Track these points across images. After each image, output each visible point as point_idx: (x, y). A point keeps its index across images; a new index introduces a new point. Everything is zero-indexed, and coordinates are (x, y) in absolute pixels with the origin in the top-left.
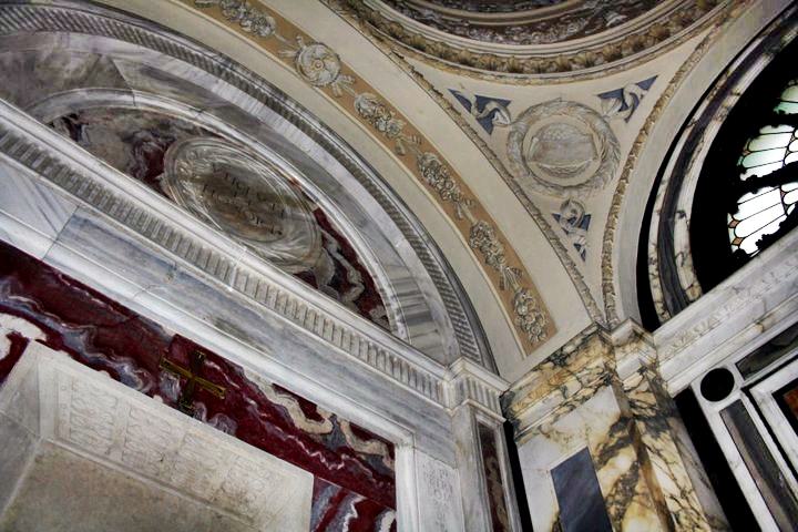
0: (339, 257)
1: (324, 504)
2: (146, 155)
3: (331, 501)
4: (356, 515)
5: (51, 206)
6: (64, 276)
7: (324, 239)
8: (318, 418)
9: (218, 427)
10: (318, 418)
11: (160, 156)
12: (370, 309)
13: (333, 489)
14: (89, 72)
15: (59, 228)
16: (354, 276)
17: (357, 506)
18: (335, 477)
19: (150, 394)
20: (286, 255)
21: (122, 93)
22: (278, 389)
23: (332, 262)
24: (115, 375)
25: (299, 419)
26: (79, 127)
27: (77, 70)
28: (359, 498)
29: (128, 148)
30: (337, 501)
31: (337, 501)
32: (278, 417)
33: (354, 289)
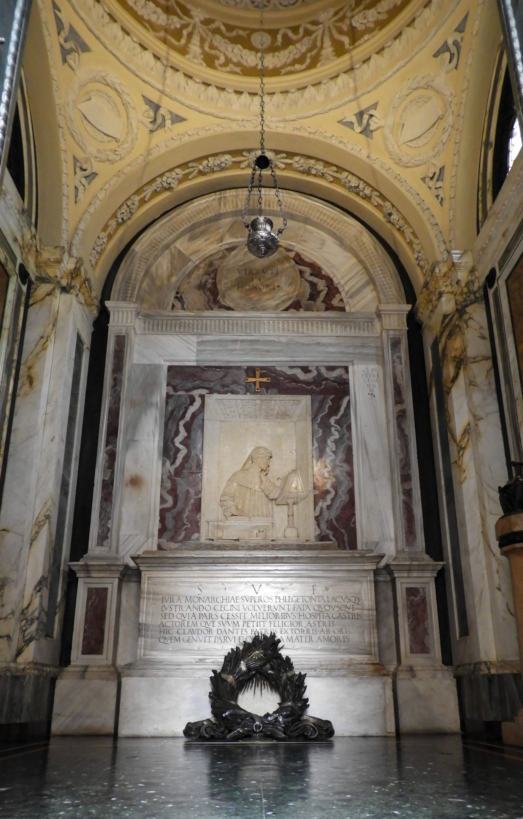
0: (312, 278)
1: (317, 405)
2: (210, 289)
3: (319, 402)
4: (331, 403)
5: (188, 343)
6: (205, 367)
7: (301, 272)
9: (271, 394)
11: (215, 284)
12: (331, 300)
13: (321, 397)
15: (195, 350)
16: (321, 285)
17: (331, 400)
18: (320, 393)
19: (245, 394)
20: (283, 298)
21: (188, 263)
22: (291, 367)
23: (308, 284)
24: (233, 392)
25: (302, 376)
26: (181, 297)
27: (168, 267)
28: (332, 397)
29: (201, 292)
30: (322, 403)
31: (322, 403)
32: (294, 379)
33: (321, 294)
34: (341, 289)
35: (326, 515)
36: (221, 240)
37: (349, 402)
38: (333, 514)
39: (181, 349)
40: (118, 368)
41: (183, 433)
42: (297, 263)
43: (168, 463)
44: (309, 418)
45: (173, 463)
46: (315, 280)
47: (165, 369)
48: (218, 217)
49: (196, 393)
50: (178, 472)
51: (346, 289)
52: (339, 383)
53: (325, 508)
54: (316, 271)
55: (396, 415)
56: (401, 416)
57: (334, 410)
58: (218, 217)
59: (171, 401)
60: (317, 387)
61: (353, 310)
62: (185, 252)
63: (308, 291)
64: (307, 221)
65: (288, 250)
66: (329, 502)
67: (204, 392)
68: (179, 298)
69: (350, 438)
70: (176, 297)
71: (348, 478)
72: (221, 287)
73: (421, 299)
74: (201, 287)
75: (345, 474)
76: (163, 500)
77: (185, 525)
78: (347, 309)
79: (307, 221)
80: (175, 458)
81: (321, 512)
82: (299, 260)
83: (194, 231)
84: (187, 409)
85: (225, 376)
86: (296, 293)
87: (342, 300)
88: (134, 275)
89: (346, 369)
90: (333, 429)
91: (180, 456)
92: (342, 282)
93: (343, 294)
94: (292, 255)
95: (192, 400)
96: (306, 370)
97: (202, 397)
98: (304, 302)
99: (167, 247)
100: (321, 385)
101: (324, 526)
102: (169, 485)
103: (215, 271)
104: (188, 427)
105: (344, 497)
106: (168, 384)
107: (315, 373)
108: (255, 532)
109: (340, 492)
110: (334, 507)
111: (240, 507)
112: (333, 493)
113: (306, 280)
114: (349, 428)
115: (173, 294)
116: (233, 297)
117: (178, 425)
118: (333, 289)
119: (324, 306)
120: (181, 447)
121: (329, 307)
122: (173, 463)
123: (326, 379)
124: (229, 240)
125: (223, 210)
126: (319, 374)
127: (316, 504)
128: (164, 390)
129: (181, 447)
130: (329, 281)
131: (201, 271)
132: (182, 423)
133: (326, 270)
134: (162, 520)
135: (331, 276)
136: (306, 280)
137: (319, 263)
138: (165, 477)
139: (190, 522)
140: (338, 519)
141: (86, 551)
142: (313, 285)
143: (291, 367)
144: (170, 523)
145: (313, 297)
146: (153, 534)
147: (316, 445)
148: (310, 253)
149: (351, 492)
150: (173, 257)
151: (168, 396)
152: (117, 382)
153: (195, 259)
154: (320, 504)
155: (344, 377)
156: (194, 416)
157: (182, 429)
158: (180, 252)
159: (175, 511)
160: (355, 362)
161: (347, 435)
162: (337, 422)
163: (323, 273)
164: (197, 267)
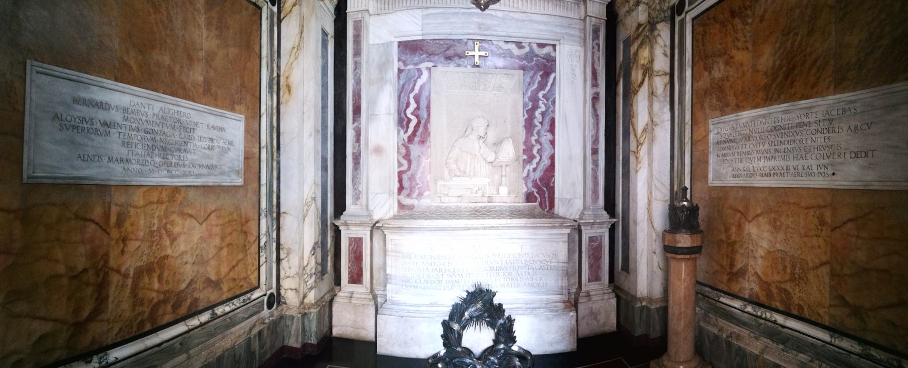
1: (528, 79)
8: (522, 47)
10: (522, 47)
13: (531, 73)
18: (532, 68)
37: (555, 78)
38: (538, 175)
44: (521, 92)
47: (396, 45)
52: (548, 60)
53: (531, 170)
56: (595, 98)
57: (542, 86)
66: (534, 166)
69: (553, 111)
81: (528, 174)
85: (448, 49)
89: (554, 46)
90: (541, 102)
101: (530, 185)
105: (546, 162)
106: (399, 60)
107: (527, 49)
108: (476, 189)
109: (544, 158)
110: (539, 170)
112: (538, 158)
114: (554, 102)
123: (537, 56)
127: (524, 167)
128: (396, 65)
147: (526, 116)
149: (552, 158)
154: (528, 167)
155: (553, 54)
160: (562, 42)
162: (544, 96)
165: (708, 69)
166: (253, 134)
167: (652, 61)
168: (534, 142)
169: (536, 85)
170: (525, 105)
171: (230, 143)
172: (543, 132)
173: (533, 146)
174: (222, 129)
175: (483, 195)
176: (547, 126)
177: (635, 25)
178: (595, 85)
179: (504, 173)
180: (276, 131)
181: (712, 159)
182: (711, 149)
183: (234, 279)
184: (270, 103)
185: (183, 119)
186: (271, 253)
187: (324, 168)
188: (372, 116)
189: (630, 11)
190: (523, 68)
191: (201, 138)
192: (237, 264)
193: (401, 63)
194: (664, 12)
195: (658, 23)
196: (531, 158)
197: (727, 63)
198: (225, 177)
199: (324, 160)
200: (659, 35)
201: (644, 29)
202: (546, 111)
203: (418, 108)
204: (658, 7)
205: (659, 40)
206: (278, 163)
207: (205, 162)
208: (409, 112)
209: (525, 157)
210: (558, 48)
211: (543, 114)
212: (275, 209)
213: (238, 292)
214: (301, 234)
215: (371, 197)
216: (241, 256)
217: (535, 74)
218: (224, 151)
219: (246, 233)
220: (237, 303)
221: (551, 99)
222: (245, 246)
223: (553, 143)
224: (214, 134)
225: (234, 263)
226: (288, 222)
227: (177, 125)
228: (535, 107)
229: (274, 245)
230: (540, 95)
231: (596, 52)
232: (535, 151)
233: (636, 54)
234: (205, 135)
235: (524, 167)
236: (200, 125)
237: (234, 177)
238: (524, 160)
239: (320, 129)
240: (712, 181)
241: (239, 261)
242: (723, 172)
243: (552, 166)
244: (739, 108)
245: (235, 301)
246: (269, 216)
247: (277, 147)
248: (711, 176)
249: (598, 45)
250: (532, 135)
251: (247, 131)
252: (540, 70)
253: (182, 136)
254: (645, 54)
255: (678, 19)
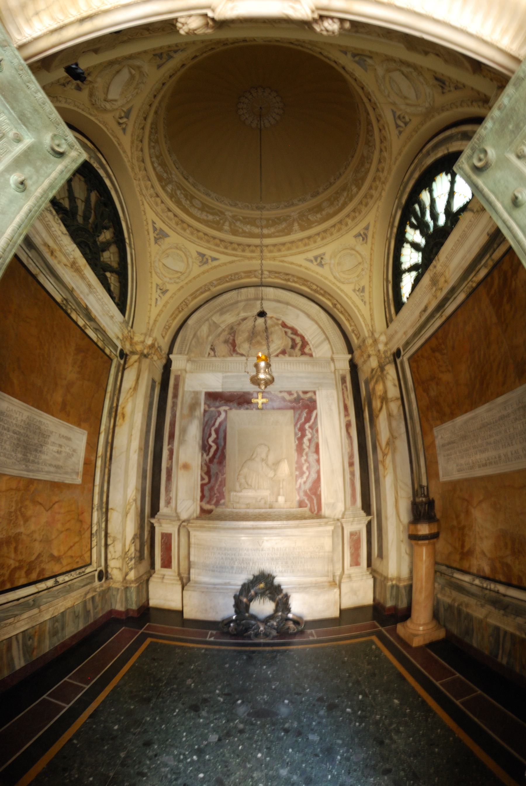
1: (297, 416)
7: (286, 333)
11: (234, 340)
14: (209, 329)
16: (298, 340)
18: (299, 408)
22: (281, 392)
31: (300, 415)
34: (309, 343)
35: (303, 487)
36: (238, 314)
39: (213, 380)
40: (175, 396)
41: (214, 436)
42: (283, 327)
43: (205, 455)
45: (208, 455)
46: (294, 337)
48: (237, 302)
49: (222, 409)
50: (211, 460)
51: (313, 343)
52: (311, 402)
54: (295, 332)
55: (345, 424)
56: (348, 425)
57: (307, 420)
58: (237, 302)
59: (207, 414)
60: (297, 404)
61: (317, 356)
62: (217, 322)
63: (290, 343)
64: (287, 304)
65: (278, 319)
66: (305, 479)
67: (227, 408)
68: (213, 349)
69: (317, 438)
70: (211, 349)
71: (317, 464)
72: (238, 342)
73: (357, 353)
74: (226, 342)
75: (315, 461)
76: (202, 479)
77: (215, 494)
78: (314, 354)
79: (287, 304)
80: (209, 451)
81: (300, 487)
82: (284, 325)
83: (222, 311)
84: (216, 419)
86: (283, 345)
87: (310, 349)
88: (187, 338)
89: (315, 393)
91: (212, 450)
92: (310, 339)
93: (311, 346)
94: (280, 322)
95: (219, 414)
96: (290, 393)
97: (226, 411)
98: (288, 350)
99: (207, 320)
100: (299, 403)
102: (205, 469)
103: (234, 333)
104: (217, 431)
105: (314, 476)
106: (205, 404)
107: (295, 395)
111: (249, 483)
112: (307, 473)
113: (289, 337)
114: (317, 431)
115: (209, 347)
116: (244, 348)
117: (210, 430)
118: (305, 343)
119: (299, 353)
120: (212, 444)
121: (303, 353)
122: (208, 455)
123: (302, 399)
124: (243, 315)
125: (239, 299)
126: (298, 396)
129: (212, 444)
130: (302, 338)
131: (226, 333)
132: (213, 429)
133: (300, 331)
134: (202, 491)
135: (303, 334)
136: (289, 337)
137: (296, 327)
138: (203, 463)
139: (219, 493)
140: (311, 489)
141: (158, 511)
142: (293, 340)
143: (281, 392)
144: (207, 493)
145: (293, 347)
146: (197, 499)
147: (297, 442)
148: (290, 322)
149: (318, 472)
150: (210, 325)
151: (205, 411)
152: (174, 404)
153: (223, 326)
155: (314, 397)
156: (220, 424)
157: (213, 433)
158: (214, 323)
159: (209, 486)
161: (316, 435)
163: (299, 333)
164: (224, 330)
165: (426, 390)
166: (92, 446)
167: (385, 392)
168: (303, 461)
169: (303, 420)
170: (296, 434)
171: (74, 451)
172: (310, 454)
173: (303, 464)
174: (69, 439)
175: (265, 503)
176: (313, 449)
177: (370, 371)
178: (347, 414)
179: (281, 486)
180: (110, 445)
181: (441, 460)
182: (438, 452)
183: (72, 557)
184: (108, 425)
185: (43, 427)
186: (100, 540)
187: (144, 477)
188: (182, 442)
189: (365, 362)
190: (293, 408)
191: (54, 443)
192: (74, 545)
193: (206, 406)
194: (388, 358)
195: (385, 365)
196: (302, 473)
197: (437, 384)
198: (67, 476)
199: (144, 471)
200: (387, 373)
201: (376, 372)
202: (312, 437)
203: (217, 438)
204: (383, 356)
205: (389, 377)
206: (110, 471)
207: (54, 463)
208: (211, 440)
209: (297, 473)
210: (317, 393)
211: (310, 440)
212: (104, 505)
213: (75, 567)
214: (124, 527)
215: (179, 502)
216: (77, 539)
217: (302, 412)
218: (69, 456)
219: (81, 521)
220: (74, 574)
221: (314, 428)
222: (80, 531)
223: (318, 461)
224: (63, 441)
225: (72, 544)
226: (115, 517)
227: (38, 431)
228: (303, 435)
229: (103, 533)
230: (307, 426)
231: (345, 392)
232: (305, 468)
233: (374, 389)
234: (57, 442)
235: (296, 481)
236: (54, 434)
237: (74, 477)
238: (296, 476)
239: (143, 448)
240: (443, 478)
241: (75, 543)
242: (451, 468)
243: (318, 481)
244: (453, 416)
245: (73, 573)
246: (100, 511)
247: (109, 459)
248: (441, 473)
249: (346, 387)
250: (302, 456)
251: (88, 443)
252: (306, 408)
253: (40, 440)
254: (380, 388)
255: (398, 361)
